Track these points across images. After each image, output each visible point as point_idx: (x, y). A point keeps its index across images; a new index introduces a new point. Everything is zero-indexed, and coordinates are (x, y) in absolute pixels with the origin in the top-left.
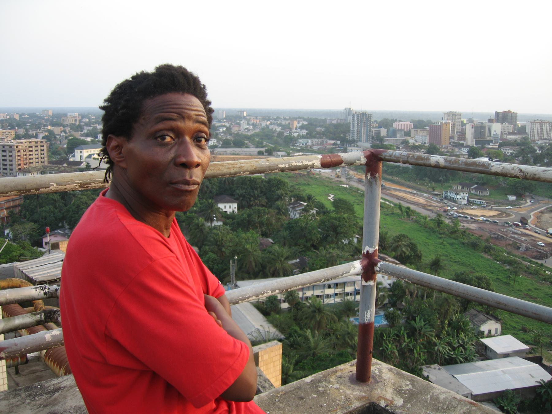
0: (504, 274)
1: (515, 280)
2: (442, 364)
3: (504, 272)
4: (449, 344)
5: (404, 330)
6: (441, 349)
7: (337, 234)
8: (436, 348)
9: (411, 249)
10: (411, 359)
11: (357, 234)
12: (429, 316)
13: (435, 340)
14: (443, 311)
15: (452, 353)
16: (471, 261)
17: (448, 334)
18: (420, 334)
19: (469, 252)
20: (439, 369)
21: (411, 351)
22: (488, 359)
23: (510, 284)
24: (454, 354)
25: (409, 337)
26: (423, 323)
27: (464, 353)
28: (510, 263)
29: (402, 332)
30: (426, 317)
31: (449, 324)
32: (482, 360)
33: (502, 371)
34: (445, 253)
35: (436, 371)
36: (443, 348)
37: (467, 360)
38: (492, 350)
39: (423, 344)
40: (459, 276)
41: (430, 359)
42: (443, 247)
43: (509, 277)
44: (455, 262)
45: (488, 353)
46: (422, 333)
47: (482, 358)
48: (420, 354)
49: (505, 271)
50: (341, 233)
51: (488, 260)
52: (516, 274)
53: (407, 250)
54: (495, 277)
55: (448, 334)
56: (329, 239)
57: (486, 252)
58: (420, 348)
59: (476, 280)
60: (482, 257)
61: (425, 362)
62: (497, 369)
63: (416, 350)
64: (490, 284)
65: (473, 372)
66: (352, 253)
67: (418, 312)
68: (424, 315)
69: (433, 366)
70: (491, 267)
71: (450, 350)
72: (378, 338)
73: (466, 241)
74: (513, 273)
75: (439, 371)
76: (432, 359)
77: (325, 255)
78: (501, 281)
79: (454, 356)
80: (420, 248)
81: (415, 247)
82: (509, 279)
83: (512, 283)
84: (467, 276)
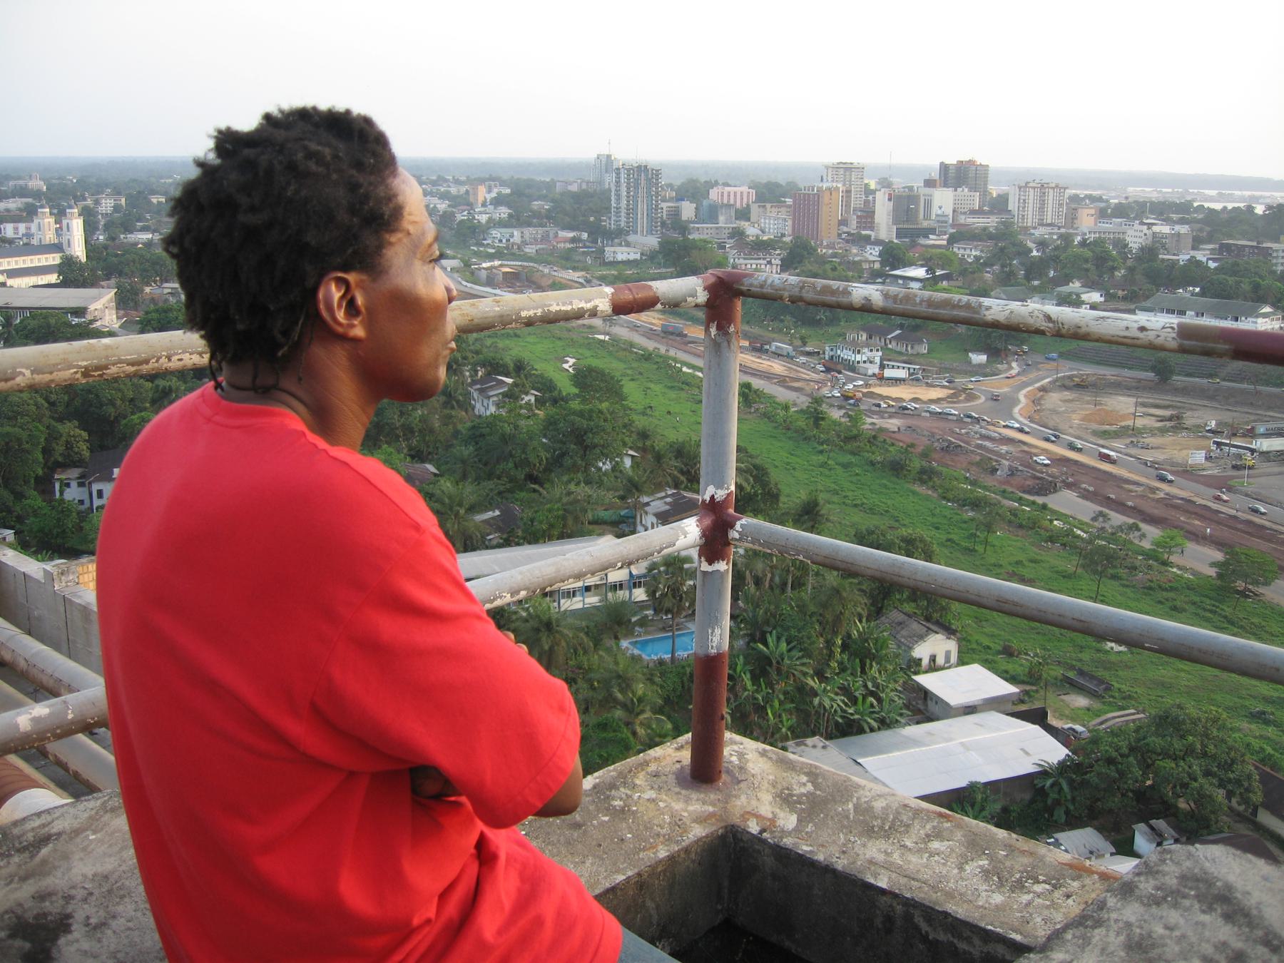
1: (986, 543)
2: (829, 737)
3: (964, 526)
4: (845, 690)
5: (745, 664)
6: (827, 703)
7: (586, 448)
8: (816, 701)
9: (755, 478)
10: (761, 728)
11: (631, 448)
12: (799, 631)
13: (812, 683)
14: (829, 617)
15: (851, 711)
16: (889, 502)
17: (843, 669)
18: (779, 671)
19: (884, 481)
20: (824, 747)
21: (761, 710)
22: (930, 719)
23: (976, 551)
24: (856, 712)
25: (755, 679)
26: (784, 646)
27: (877, 709)
28: (976, 504)
29: (739, 668)
30: (793, 632)
31: (845, 647)
32: (918, 723)
33: (962, 744)
35: (818, 752)
36: (833, 700)
37: (885, 724)
38: (938, 700)
39: (785, 693)
41: (804, 726)
42: (827, 472)
44: (856, 506)
45: (931, 704)
46: (785, 669)
47: (918, 717)
48: (780, 716)
49: (965, 522)
50: (595, 446)
51: (928, 498)
52: (989, 528)
53: (747, 480)
54: (944, 537)
55: (843, 669)
56: (568, 461)
57: (923, 482)
58: (781, 703)
60: (914, 493)
61: (793, 732)
62: (951, 740)
63: (772, 706)
64: (932, 552)
65: (898, 750)
66: (621, 493)
67: (772, 620)
68: (788, 629)
69: (810, 741)
70: (933, 515)
71: (846, 705)
72: (686, 684)
74: (983, 527)
75: (824, 752)
76: (808, 725)
77: (561, 498)
78: (957, 544)
79: (856, 717)
80: (775, 476)
83: (980, 548)
84: (882, 538)
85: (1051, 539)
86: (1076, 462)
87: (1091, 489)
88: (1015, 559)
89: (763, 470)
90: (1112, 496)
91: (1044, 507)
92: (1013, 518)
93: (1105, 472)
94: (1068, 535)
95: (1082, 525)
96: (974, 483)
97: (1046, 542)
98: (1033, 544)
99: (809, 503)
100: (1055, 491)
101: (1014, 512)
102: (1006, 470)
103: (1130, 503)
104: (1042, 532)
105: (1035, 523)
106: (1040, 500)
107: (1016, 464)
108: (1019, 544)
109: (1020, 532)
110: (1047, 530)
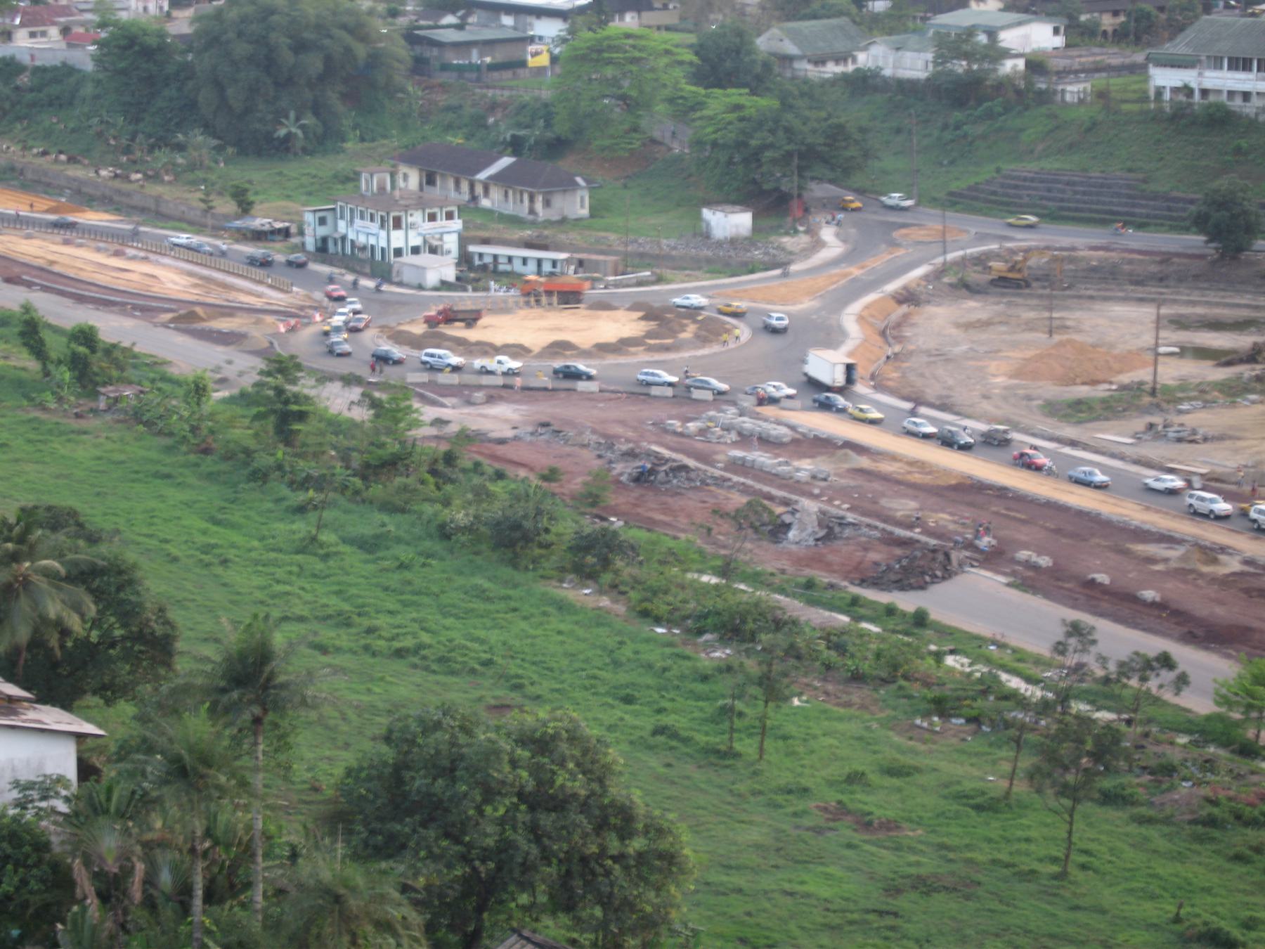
0: (699, 698)
3: (700, 687)
16: (494, 637)
19: (479, 581)
23: (737, 755)
34: (335, 603)
40: (413, 742)
42: (320, 566)
43: (727, 712)
44: (400, 653)
49: (705, 678)
51: (600, 619)
52: (772, 690)
54: (648, 723)
57: (587, 575)
59: (523, 753)
60: (563, 607)
64: (607, 768)
70: (617, 664)
73: (461, 517)
78: (686, 741)
81: (120, 588)
82: (732, 730)
83: (748, 746)
85: (942, 707)
86: (1002, 493)
87: (1045, 561)
88: (837, 771)
89: (120, 572)
90: (1103, 578)
91: (920, 619)
92: (833, 655)
93: (1081, 514)
94: (985, 693)
95: (1021, 662)
96: (725, 571)
97: (926, 715)
98: (891, 724)
99: (242, 656)
100: (948, 574)
101: (835, 639)
102: (812, 524)
103: (1149, 594)
104: (916, 689)
105: (895, 667)
106: (907, 602)
107: (840, 508)
108: (853, 728)
109: (857, 694)
110: (927, 684)
